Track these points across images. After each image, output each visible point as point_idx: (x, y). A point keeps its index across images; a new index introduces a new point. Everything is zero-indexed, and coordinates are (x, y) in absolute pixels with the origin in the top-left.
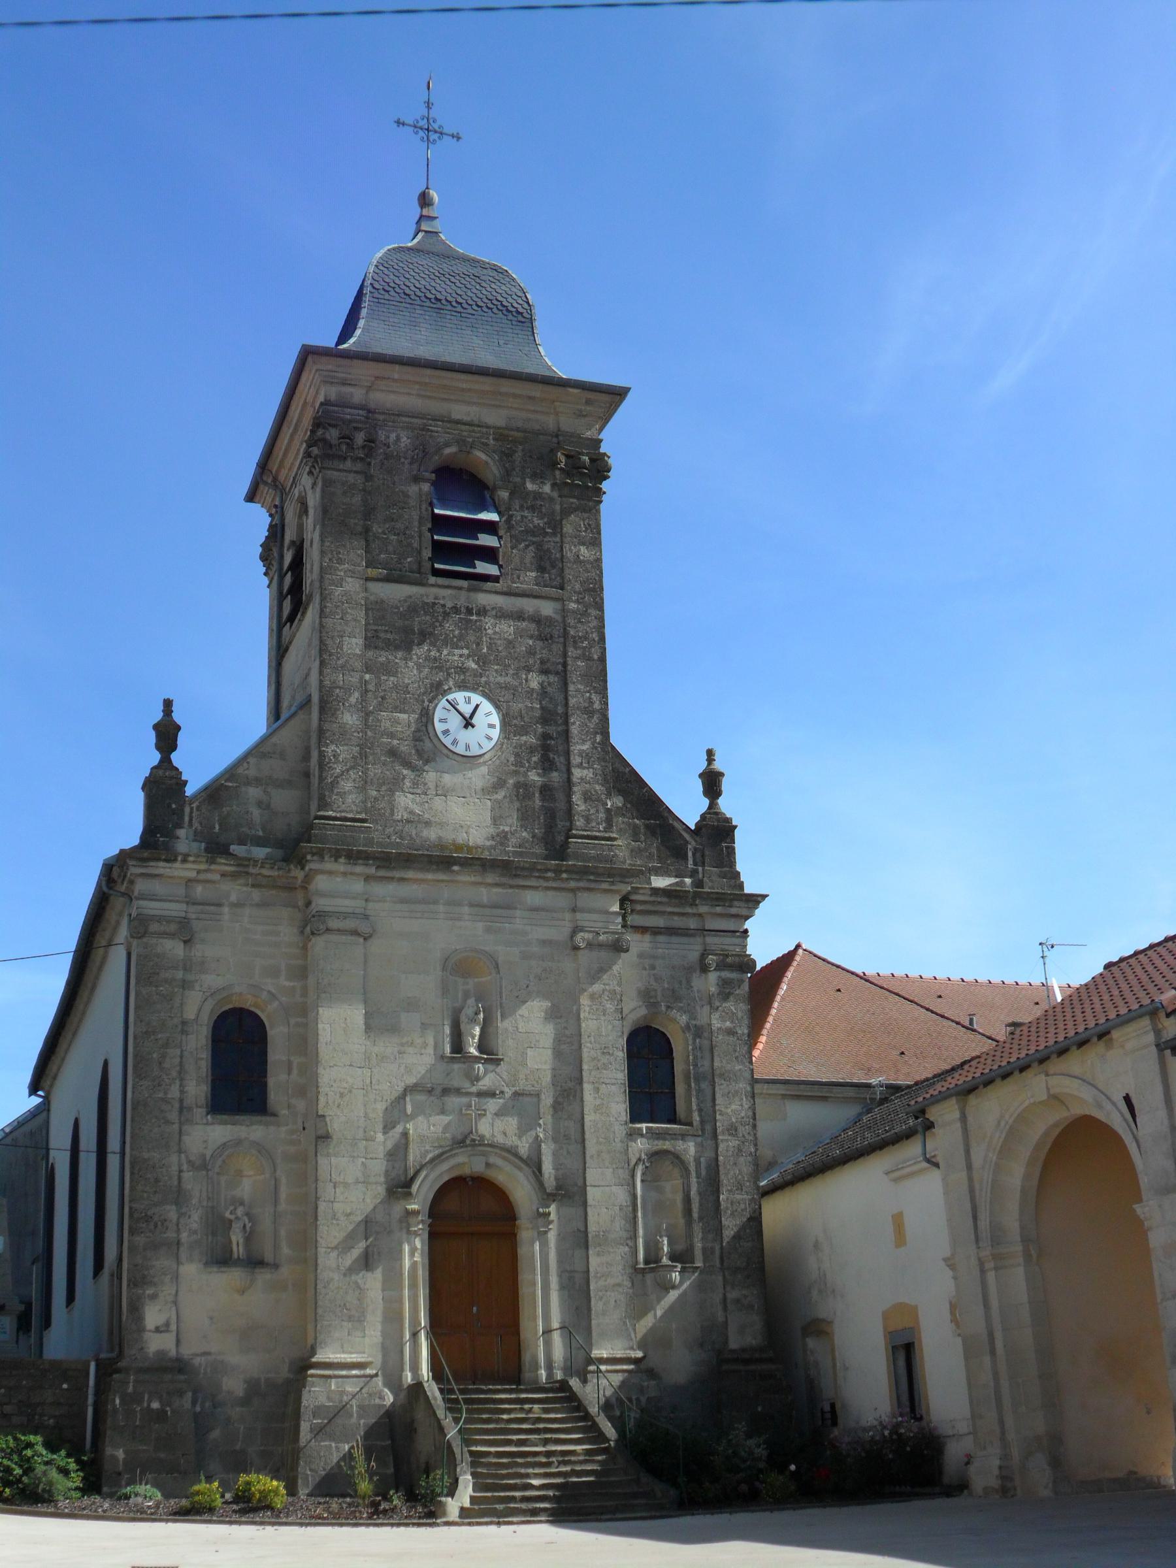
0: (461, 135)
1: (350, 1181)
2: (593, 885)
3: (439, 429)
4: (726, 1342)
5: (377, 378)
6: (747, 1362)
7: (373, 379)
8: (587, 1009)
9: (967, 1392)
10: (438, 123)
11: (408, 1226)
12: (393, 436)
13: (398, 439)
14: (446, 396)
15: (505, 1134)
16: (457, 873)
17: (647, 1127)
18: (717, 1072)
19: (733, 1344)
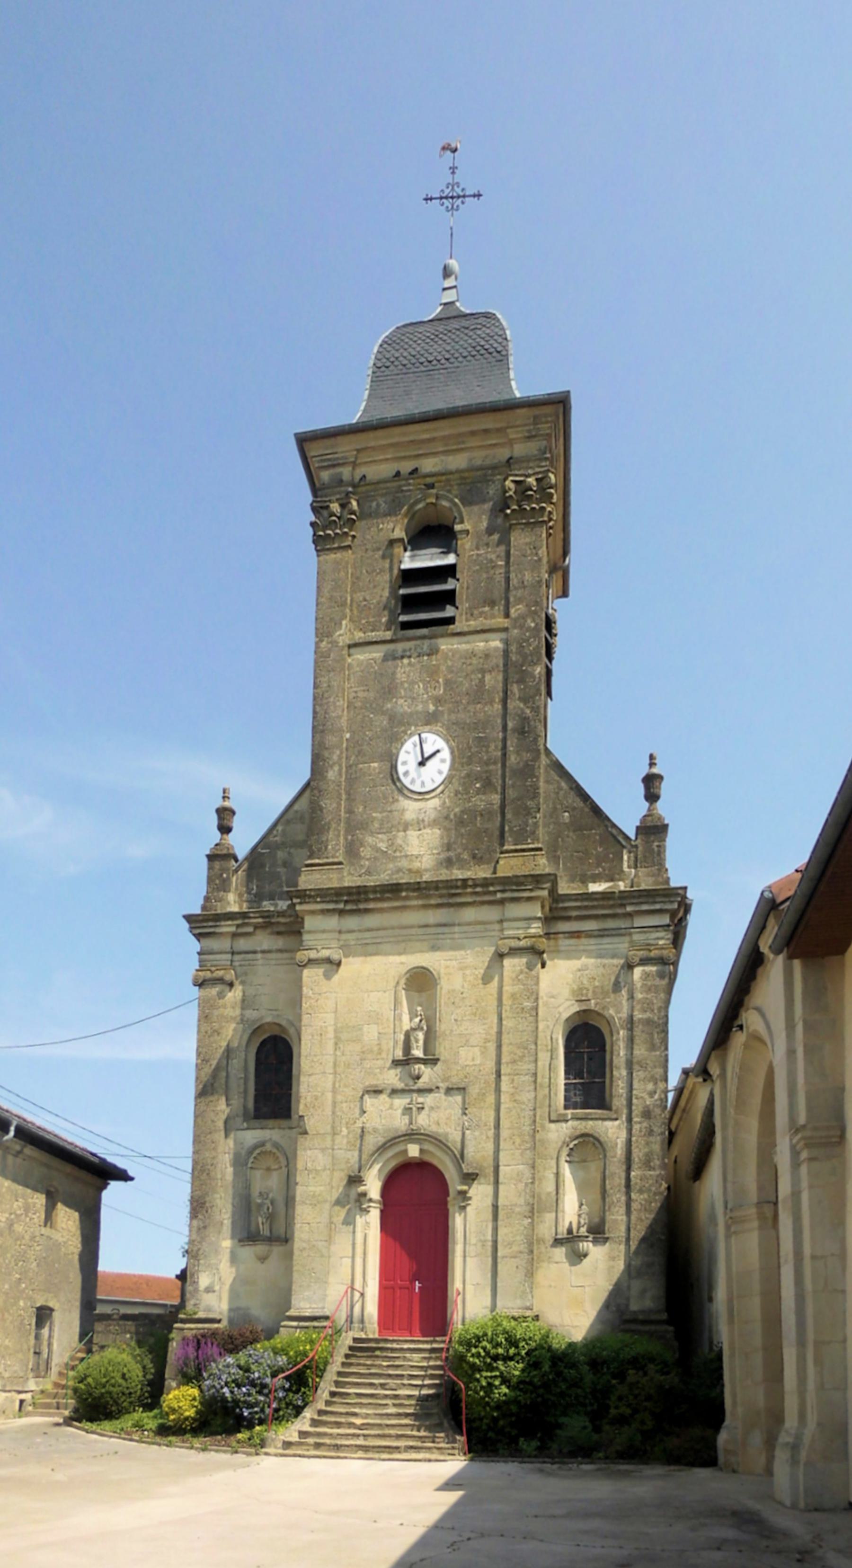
0: (481, 193)
1: (319, 1168)
2: (516, 895)
3: (411, 488)
4: (627, 1306)
5: (358, 451)
6: (644, 1322)
7: (355, 453)
8: (508, 1008)
9: (295, 1276)
10: (461, 187)
11: (361, 1204)
12: (374, 504)
13: (378, 505)
14: (416, 453)
15: (438, 1124)
16: (406, 898)
17: (572, 1114)
18: (635, 1060)
19: (634, 1306)
